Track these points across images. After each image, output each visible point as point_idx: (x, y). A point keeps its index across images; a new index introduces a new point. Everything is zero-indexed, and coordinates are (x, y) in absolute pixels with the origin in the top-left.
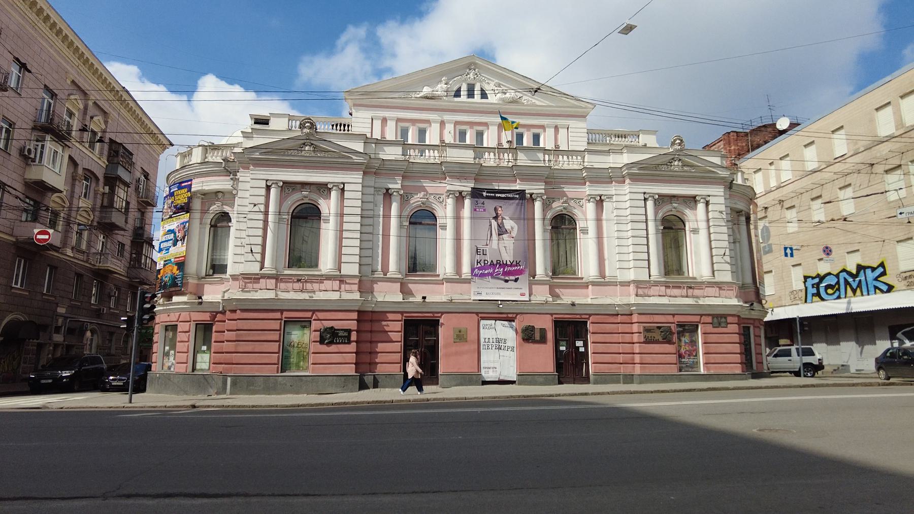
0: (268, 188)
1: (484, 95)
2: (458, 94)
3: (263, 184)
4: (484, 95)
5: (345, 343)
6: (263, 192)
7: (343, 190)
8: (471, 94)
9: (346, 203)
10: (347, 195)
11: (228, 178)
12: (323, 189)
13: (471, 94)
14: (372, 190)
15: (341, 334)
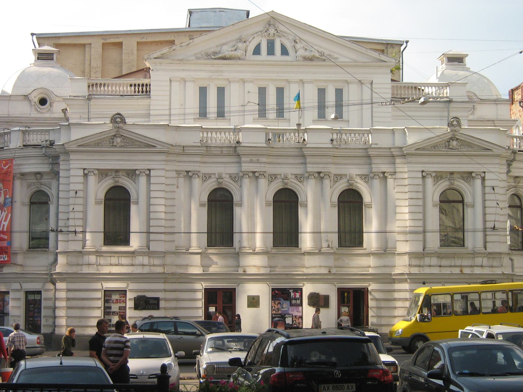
0: (86, 175)
1: (284, 51)
2: (257, 51)
3: (81, 172)
4: (284, 51)
5: (155, 309)
6: (81, 179)
7: (149, 176)
8: (271, 51)
9: (153, 187)
10: (153, 180)
11: (46, 162)
12: (132, 174)
13: (271, 51)
14: (174, 174)
15: (151, 302)
